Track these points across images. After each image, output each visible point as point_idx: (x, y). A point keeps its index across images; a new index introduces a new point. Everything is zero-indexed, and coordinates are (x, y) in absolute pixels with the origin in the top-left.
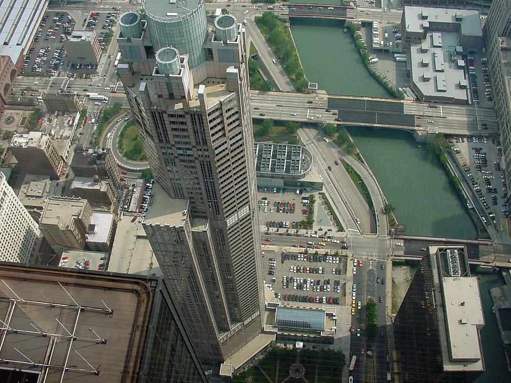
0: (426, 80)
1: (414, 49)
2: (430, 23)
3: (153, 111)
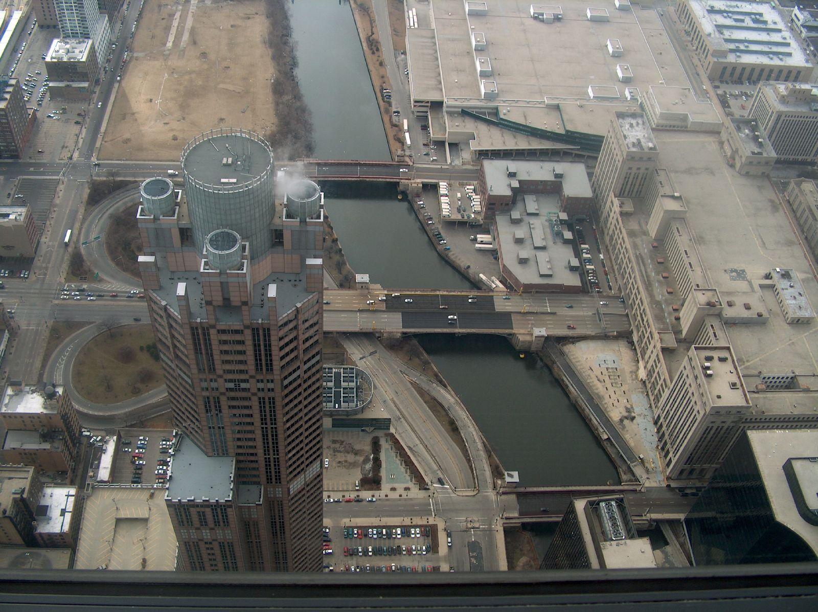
0: (523, 262)
1: (501, 222)
2: (520, 182)
3: (195, 326)
